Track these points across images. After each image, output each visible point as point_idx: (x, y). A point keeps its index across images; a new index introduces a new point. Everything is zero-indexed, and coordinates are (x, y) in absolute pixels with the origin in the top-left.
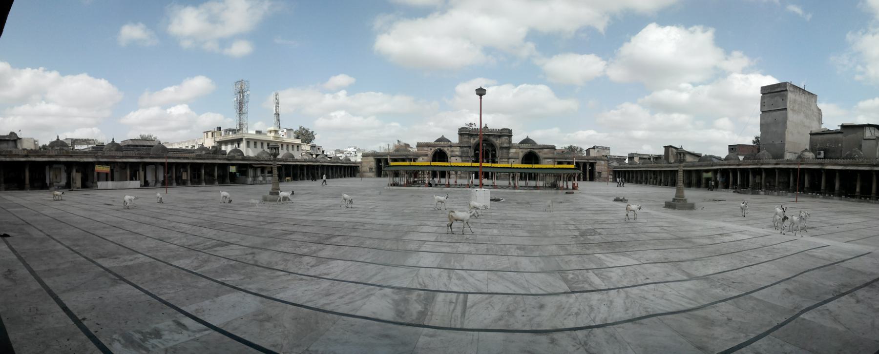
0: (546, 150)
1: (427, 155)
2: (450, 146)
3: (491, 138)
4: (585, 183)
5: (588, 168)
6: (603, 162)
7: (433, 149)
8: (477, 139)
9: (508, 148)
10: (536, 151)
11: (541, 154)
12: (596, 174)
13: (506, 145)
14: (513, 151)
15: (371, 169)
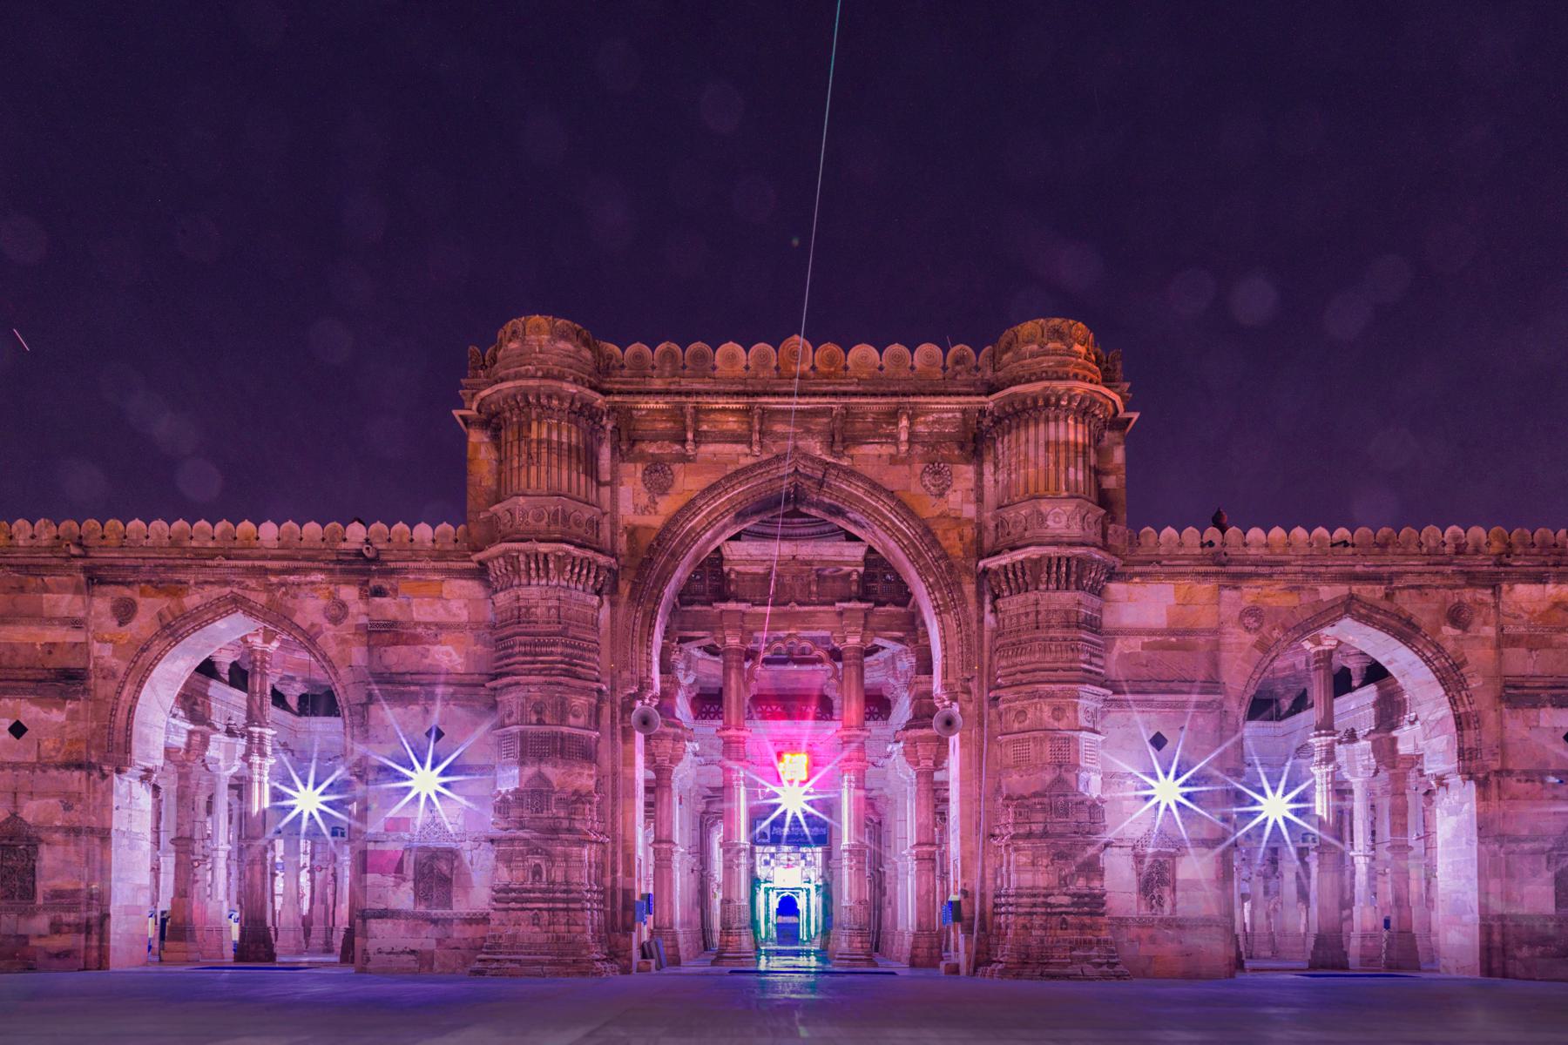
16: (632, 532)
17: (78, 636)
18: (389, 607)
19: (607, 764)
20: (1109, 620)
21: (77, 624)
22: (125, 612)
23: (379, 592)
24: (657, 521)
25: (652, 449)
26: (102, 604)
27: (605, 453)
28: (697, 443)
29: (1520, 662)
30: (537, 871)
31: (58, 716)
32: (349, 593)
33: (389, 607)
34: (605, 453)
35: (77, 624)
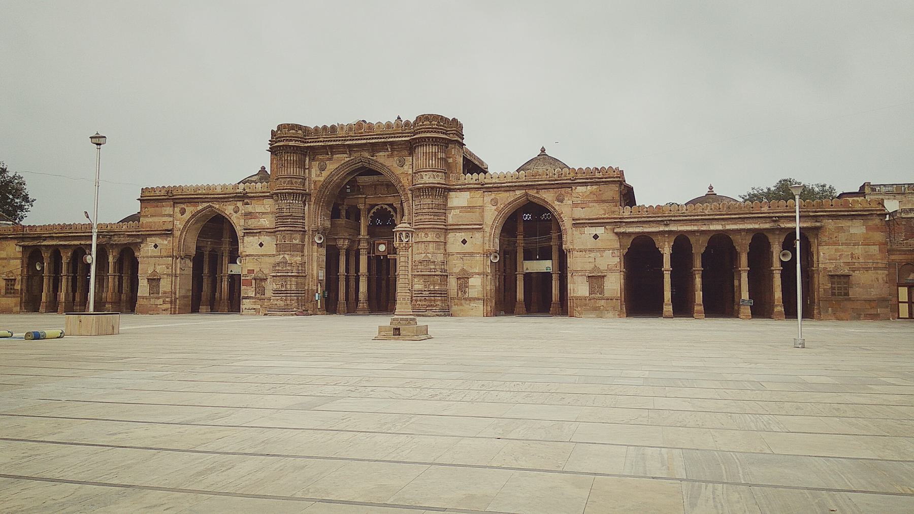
0: (580, 189)
1: (167, 233)
2: (243, 197)
3: (382, 157)
4: (682, 323)
5: (778, 255)
6: (857, 229)
7: (190, 210)
8: (331, 167)
9: (445, 191)
10: (548, 196)
11: (566, 209)
12: (822, 284)
13: (428, 179)
14: (458, 200)
15: (10, 282)
16: (315, 182)
17: (171, 219)
18: (249, 208)
19: (306, 253)
20: (449, 205)
21: (170, 216)
22: (183, 212)
23: (247, 204)
24: (322, 179)
25: (320, 157)
26: (177, 210)
27: (307, 159)
28: (332, 155)
29: (580, 213)
30: (282, 286)
31: (166, 242)
32: (239, 204)
33: (249, 208)
34: (307, 161)
35: (170, 216)
